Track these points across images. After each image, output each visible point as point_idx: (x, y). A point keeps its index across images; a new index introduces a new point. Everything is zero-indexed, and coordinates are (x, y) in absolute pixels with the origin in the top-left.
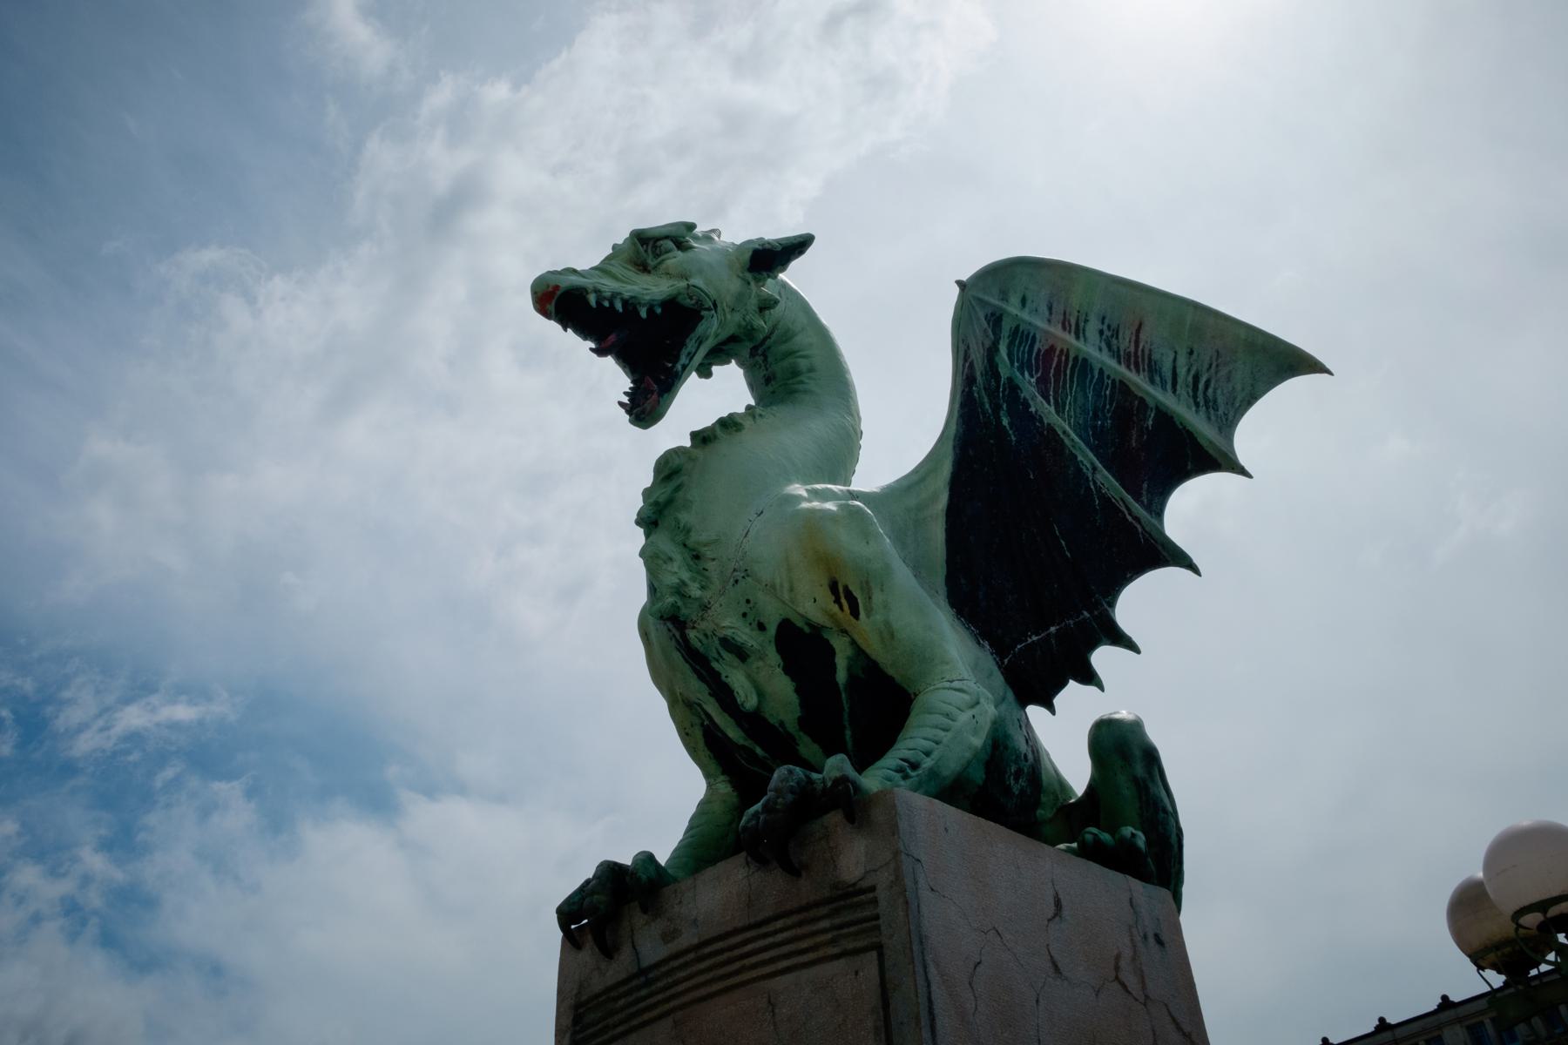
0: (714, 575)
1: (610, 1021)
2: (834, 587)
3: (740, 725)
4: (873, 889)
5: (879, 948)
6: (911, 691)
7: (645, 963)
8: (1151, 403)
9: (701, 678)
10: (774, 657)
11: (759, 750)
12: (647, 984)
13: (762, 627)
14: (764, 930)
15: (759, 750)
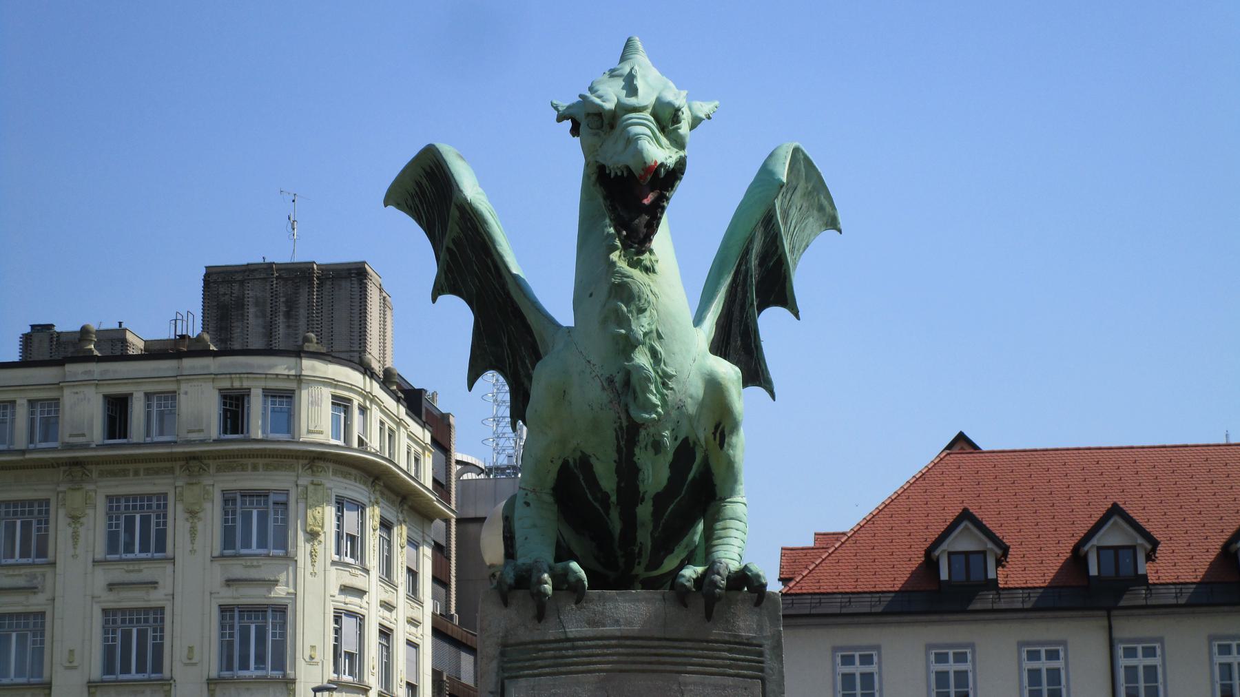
0: (670, 398)
1: (540, 663)
2: (717, 427)
3: (619, 483)
4: (760, 646)
5: (763, 680)
6: (719, 495)
7: (571, 635)
8: (779, 252)
9: (619, 450)
10: (670, 457)
11: (614, 498)
12: (573, 648)
13: (676, 439)
14: (676, 644)
15: (614, 498)
